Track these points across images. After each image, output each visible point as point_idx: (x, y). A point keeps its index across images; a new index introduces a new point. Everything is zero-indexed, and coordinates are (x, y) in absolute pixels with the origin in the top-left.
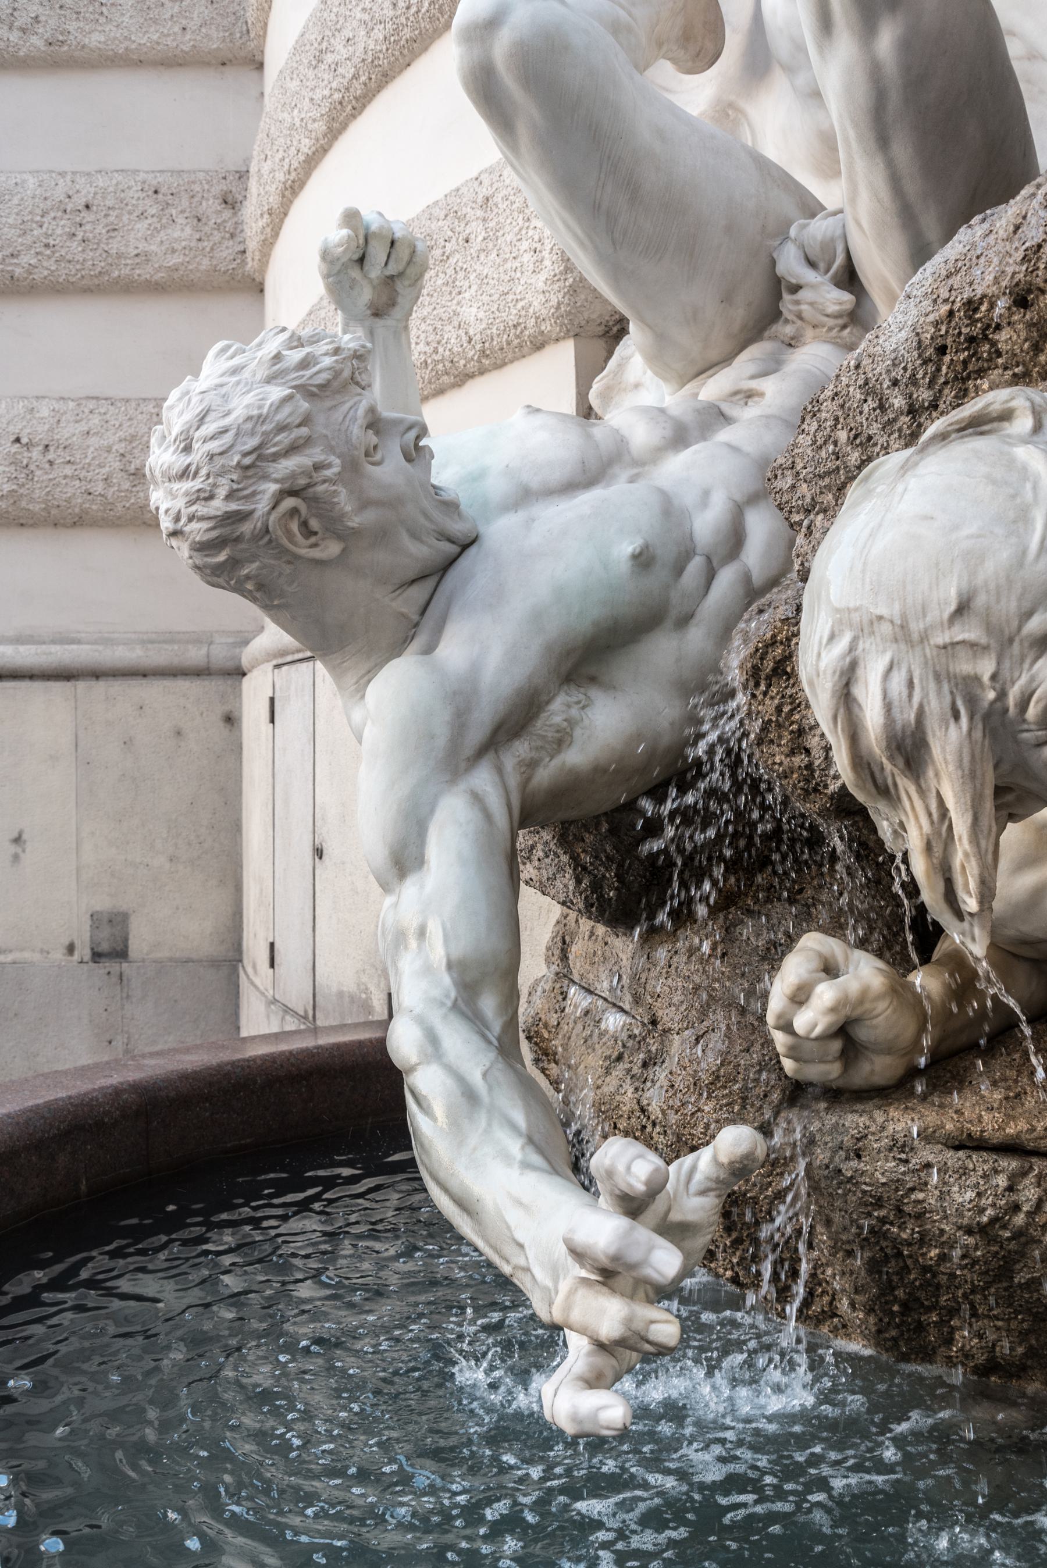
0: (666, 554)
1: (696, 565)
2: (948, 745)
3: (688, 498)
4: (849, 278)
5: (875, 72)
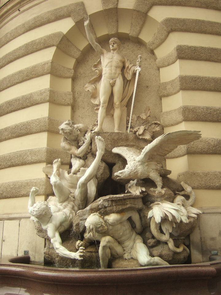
0: (66, 217)
1: (68, 217)
2: (94, 229)
3: (67, 213)
4: (74, 198)
5: (82, 190)
